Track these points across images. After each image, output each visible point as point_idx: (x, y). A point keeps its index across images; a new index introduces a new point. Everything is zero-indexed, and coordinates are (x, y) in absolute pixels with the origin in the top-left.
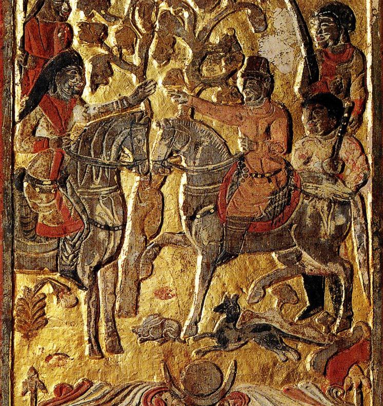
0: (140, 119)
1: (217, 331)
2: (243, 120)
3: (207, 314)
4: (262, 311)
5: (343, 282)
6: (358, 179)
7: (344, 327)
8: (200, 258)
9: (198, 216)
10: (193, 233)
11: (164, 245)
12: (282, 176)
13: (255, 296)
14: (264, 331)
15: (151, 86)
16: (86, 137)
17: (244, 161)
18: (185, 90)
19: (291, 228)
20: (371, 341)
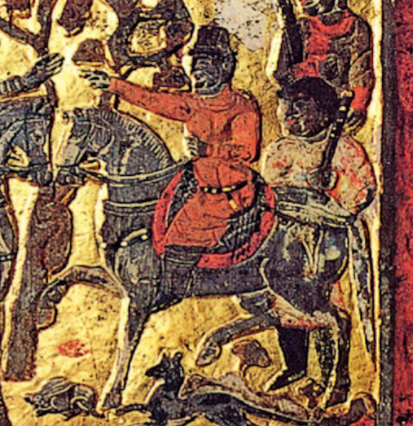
0: (40, 107)
1: (150, 403)
2: (191, 114)
3: (137, 374)
4: (217, 375)
5: (335, 338)
6: (359, 197)
7: (338, 398)
8: (125, 302)
9: (124, 244)
10: (117, 267)
11: (74, 283)
12: (248, 192)
13: (207, 355)
14: (219, 402)
15: (56, 62)
17: (192, 170)
18: (106, 69)
19: (259, 264)
20: (375, 419)
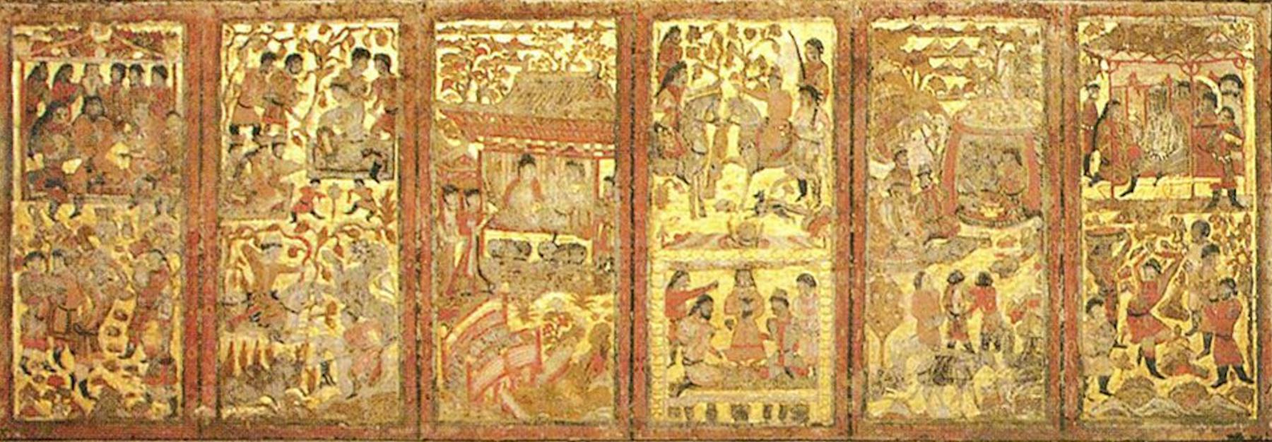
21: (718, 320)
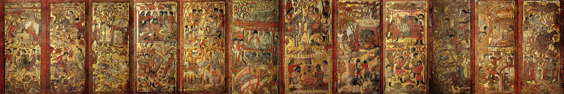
16: (294, 18)
21: (302, 72)
